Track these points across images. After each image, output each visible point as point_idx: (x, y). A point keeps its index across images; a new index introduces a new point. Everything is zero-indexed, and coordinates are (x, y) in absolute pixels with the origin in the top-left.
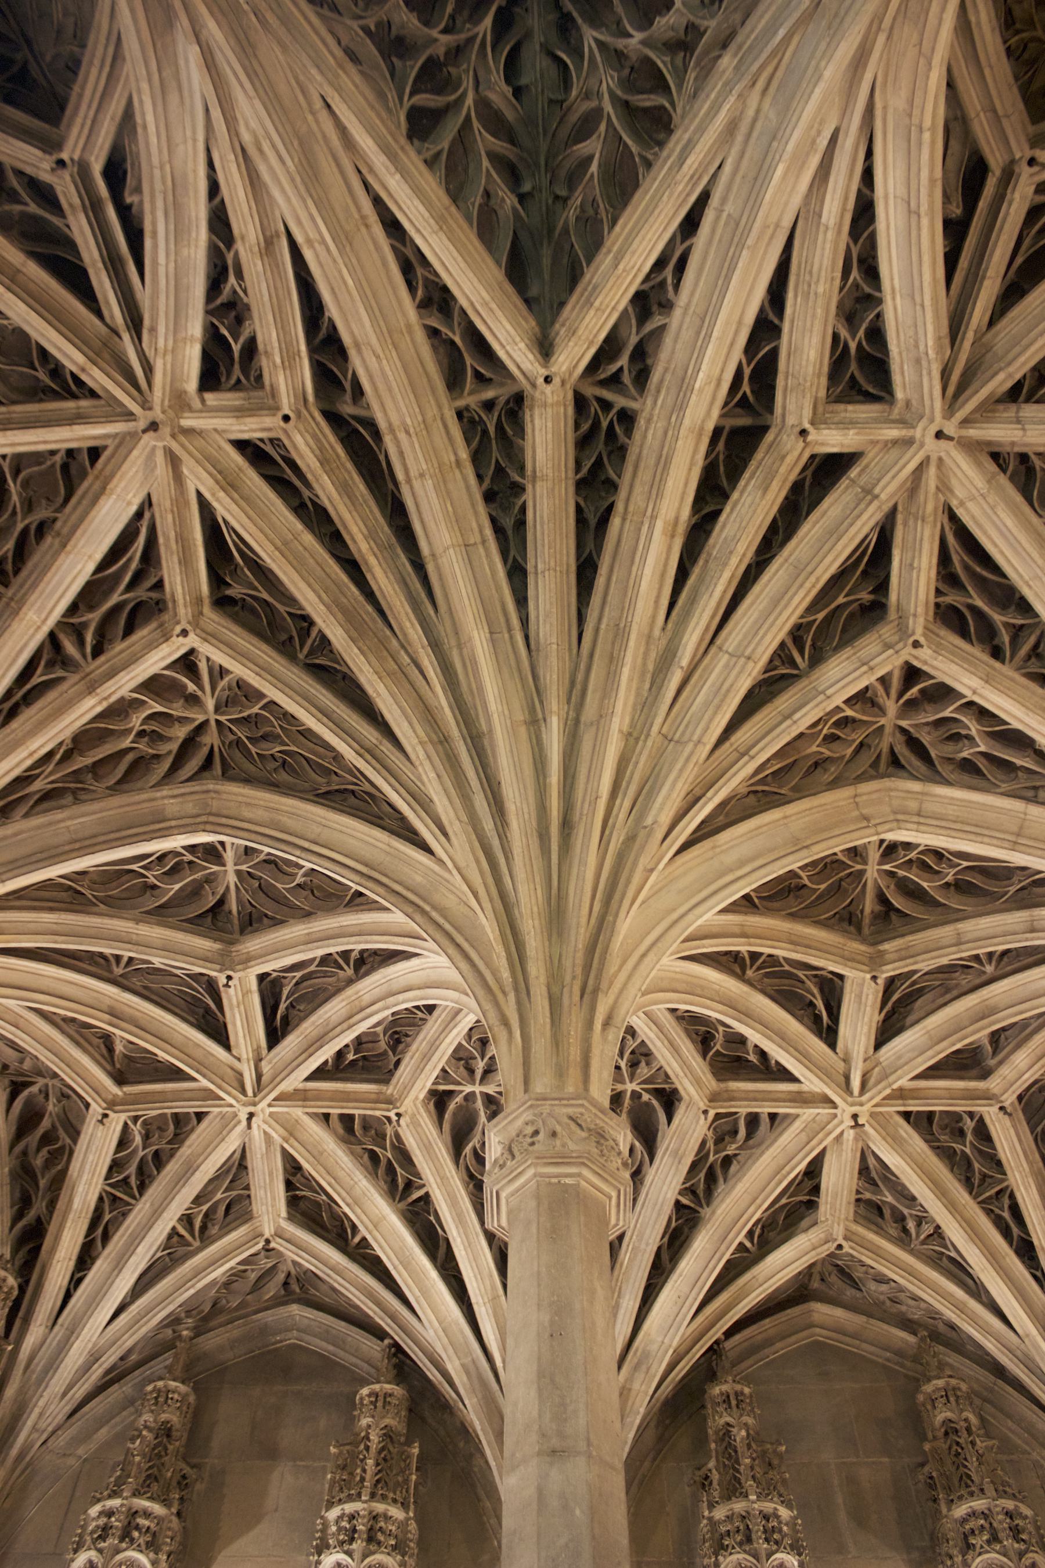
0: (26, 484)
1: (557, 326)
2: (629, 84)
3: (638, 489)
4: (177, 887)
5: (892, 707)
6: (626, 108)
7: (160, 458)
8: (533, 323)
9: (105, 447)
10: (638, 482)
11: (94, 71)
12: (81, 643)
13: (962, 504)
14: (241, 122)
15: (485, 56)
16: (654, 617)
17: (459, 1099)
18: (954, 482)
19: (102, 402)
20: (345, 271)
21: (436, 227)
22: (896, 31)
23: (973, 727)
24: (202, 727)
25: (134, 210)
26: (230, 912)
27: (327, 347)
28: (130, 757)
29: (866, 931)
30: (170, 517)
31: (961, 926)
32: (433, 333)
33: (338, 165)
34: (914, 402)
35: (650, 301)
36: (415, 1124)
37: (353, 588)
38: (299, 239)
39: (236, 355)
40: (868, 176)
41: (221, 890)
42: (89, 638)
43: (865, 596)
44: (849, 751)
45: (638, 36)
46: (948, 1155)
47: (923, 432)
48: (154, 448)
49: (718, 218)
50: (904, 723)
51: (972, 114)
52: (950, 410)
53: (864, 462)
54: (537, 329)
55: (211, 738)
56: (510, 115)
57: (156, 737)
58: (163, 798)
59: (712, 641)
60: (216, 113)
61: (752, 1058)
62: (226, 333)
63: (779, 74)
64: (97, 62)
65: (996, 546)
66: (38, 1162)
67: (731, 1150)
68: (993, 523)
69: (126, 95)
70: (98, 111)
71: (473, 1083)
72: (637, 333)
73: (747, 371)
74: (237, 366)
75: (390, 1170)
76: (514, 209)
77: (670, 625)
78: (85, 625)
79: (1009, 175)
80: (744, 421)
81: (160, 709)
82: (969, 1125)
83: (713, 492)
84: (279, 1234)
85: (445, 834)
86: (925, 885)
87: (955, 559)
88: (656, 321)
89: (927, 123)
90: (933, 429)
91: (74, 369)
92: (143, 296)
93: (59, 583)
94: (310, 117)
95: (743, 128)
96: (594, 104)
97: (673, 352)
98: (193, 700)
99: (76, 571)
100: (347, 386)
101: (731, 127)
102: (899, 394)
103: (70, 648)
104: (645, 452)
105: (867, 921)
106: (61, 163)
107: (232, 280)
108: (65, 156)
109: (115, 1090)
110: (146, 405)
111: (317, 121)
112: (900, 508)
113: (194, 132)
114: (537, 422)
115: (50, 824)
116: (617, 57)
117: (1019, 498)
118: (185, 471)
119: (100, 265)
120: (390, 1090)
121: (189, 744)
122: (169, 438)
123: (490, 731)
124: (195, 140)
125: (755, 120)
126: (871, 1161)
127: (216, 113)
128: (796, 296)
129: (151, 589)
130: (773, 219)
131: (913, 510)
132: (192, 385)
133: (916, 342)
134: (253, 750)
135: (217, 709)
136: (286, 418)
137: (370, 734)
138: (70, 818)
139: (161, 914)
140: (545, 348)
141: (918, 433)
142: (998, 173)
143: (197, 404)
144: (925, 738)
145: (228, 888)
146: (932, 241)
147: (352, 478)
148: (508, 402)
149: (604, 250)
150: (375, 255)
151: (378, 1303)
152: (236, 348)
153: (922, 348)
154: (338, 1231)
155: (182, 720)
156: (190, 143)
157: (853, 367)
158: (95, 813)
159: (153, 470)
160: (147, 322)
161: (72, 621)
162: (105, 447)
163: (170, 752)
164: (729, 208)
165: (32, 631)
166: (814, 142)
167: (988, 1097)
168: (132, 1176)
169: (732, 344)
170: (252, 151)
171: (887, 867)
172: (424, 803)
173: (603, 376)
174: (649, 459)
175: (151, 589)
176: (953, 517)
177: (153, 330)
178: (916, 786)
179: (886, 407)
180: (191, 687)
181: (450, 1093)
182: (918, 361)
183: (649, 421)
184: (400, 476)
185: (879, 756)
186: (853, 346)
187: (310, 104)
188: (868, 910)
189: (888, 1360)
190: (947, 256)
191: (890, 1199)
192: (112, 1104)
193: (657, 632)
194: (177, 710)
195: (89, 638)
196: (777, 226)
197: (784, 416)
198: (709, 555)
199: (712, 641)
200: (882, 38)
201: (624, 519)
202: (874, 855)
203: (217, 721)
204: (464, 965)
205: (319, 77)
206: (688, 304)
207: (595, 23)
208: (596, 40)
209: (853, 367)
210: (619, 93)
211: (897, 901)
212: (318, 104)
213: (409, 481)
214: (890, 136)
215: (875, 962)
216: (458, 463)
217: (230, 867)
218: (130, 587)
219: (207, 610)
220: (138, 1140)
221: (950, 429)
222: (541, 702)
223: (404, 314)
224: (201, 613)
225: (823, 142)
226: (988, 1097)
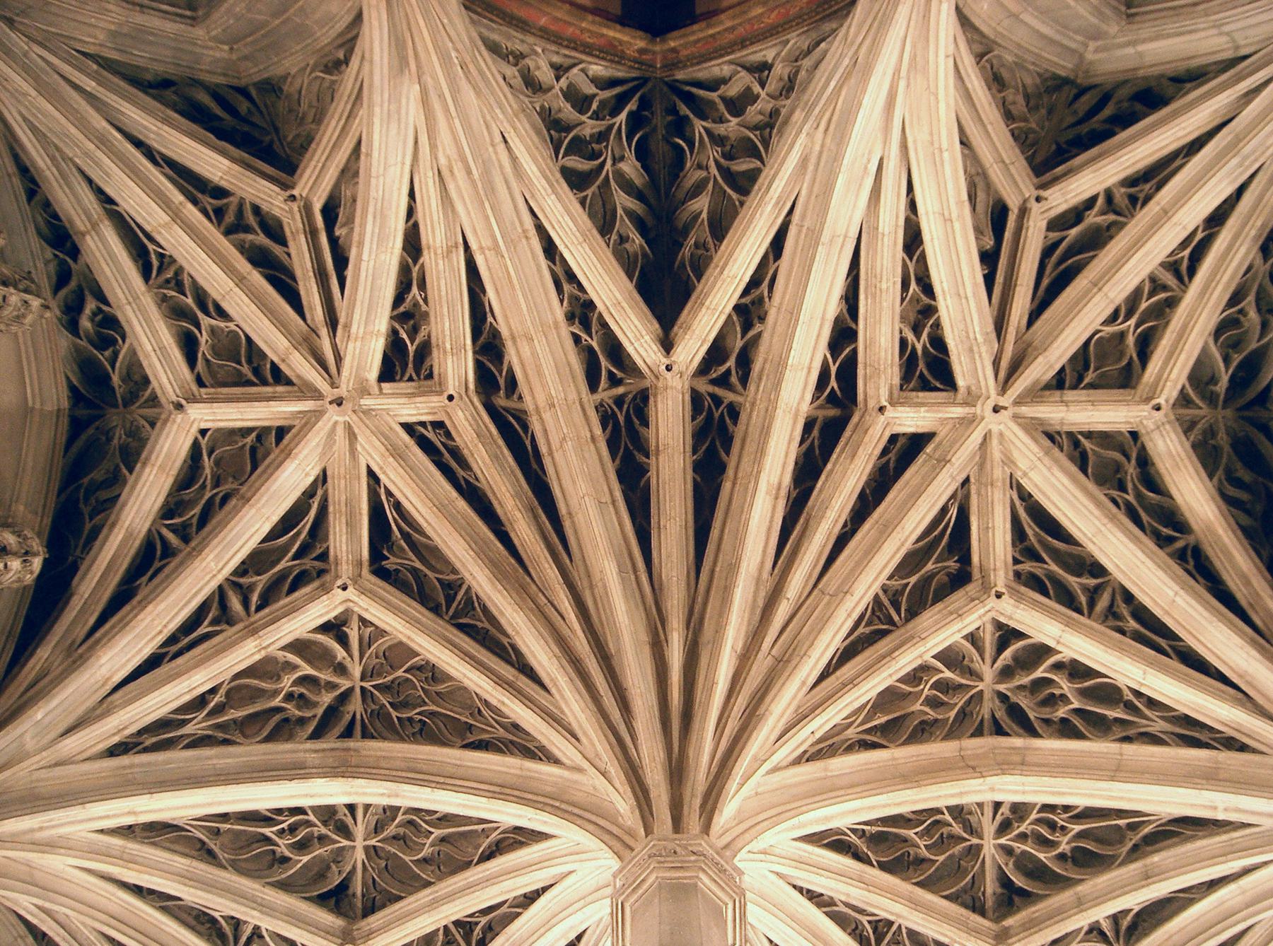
0: (217, 463)
1: (676, 328)
2: (729, 156)
3: (745, 459)
4: (305, 859)
5: (988, 673)
6: (728, 174)
7: (340, 431)
8: (657, 326)
9: (290, 428)
10: (745, 452)
11: (333, 123)
12: (246, 603)
13: (1025, 474)
14: (440, 148)
15: (621, 138)
16: (762, 563)
18: (1016, 455)
19: (296, 388)
20: (509, 263)
21: (581, 239)
22: (912, 81)
23: (1064, 685)
24: (345, 696)
25: (341, 241)
26: (354, 895)
27: (489, 346)
28: (277, 718)
29: (990, 913)
30: (343, 482)
31: (1079, 888)
32: (577, 339)
33: (509, 188)
34: (973, 388)
35: (749, 311)
37: (499, 545)
38: (474, 246)
39: (411, 354)
40: (912, 206)
41: (348, 868)
42: (255, 598)
43: (952, 564)
44: (953, 714)
45: (734, 121)
47: (984, 409)
48: (336, 423)
49: (800, 232)
50: (1002, 688)
51: (988, 165)
52: (1003, 389)
53: (937, 440)
54: (660, 331)
55: (355, 705)
57: (302, 701)
58: (306, 751)
59: (815, 586)
60: (423, 139)
62: (405, 336)
63: (835, 118)
64: (336, 117)
65: (1057, 507)
68: (1053, 486)
69: (357, 134)
70: (327, 159)
72: (742, 337)
73: (833, 369)
74: (411, 365)
76: (641, 246)
77: (776, 571)
78: (251, 588)
79: (1024, 211)
80: (833, 412)
81: (309, 670)
83: (809, 470)
85: (577, 739)
86: (1041, 856)
87: (1029, 532)
88: (758, 328)
89: (945, 145)
90: (990, 405)
91: (276, 360)
92: (341, 306)
93: (238, 536)
94: (491, 149)
95: (813, 160)
96: (704, 174)
97: (770, 345)
98: (341, 669)
99: (253, 530)
100: (502, 382)
101: (804, 162)
102: (961, 382)
103: (235, 604)
104: (750, 429)
105: (990, 903)
106: (293, 198)
107: (415, 290)
108: (296, 192)
110: (333, 385)
111: (496, 153)
112: (972, 480)
113: (404, 158)
114: (660, 405)
115: (198, 759)
116: (718, 140)
117: (1074, 469)
118: (359, 448)
119: (311, 274)
121: (332, 713)
122: (350, 413)
123: (619, 651)
124: (403, 164)
125: (821, 153)
127: (423, 139)
128: (866, 298)
129: (316, 559)
130: (841, 230)
131: (984, 480)
132: (373, 374)
133: (967, 332)
134: (394, 714)
135: (362, 680)
136: (451, 398)
137: (508, 672)
138: (217, 757)
139: (284, 886)
140: (667, 345)
141: (978, 410)
142: (1016, 211)
143: (376, 390)
144: (1024, 702)
145: (354, 868)
146: (973, 272)
147: (502, 452)
148: (635, 398)
149: (712, 265)
150: (532, 263)
152: (411, 349)
153: (972, 336)
155: (331, 686)
156: (399, 165)
157: (921, 366)
158: (240, 756)
159: (331, 447)
160: (342, 320)
161: (242, 580)
162: (290, 428)
163: (315, 716)
164: (807, 224)
165: (207, 578)
166: (866, 168)
169: (818, 336)
170: (445, 173)
171: (1003, 841)
172: (555, 719)
173: (714, 376)
174: (754, 433)
175: (316, 559)
176: (1025, 496)
177: (347, 326)
178: (1017, 742)
179: (951, 394)
180: (340, 653)
182: (971, 350)
183: (753, 404)
184: (543, 449)
185: (982, 721)
186: (919, 347)
187: (492, 140)
188: (989, 891)
190: (985, 276)
193: (765, 575)
194: (325, 676)
195: (255, 598)
197: (866, 400)
198: (809, 515)
199: (815, 586)
200: (902, 84)
201: (734, 484)
202: (989, 827)
203: (362, 688)
204: (591, 827)
205: (501, 116)
206: (781, 304)
207: (703, 117)
208: (705, 128)
209: (921, 366)
210: (722, 161)
211: (1019, 881)
212: (498, 139)
213: (551, 453)
214: (922, 164)
216: (593, 439)
217: (359, 843)
218: (295, 558)
219: (365, 571)
221: (1005, 401)
222: (664, 629)
223: (553, 314)
224: (360, 575)
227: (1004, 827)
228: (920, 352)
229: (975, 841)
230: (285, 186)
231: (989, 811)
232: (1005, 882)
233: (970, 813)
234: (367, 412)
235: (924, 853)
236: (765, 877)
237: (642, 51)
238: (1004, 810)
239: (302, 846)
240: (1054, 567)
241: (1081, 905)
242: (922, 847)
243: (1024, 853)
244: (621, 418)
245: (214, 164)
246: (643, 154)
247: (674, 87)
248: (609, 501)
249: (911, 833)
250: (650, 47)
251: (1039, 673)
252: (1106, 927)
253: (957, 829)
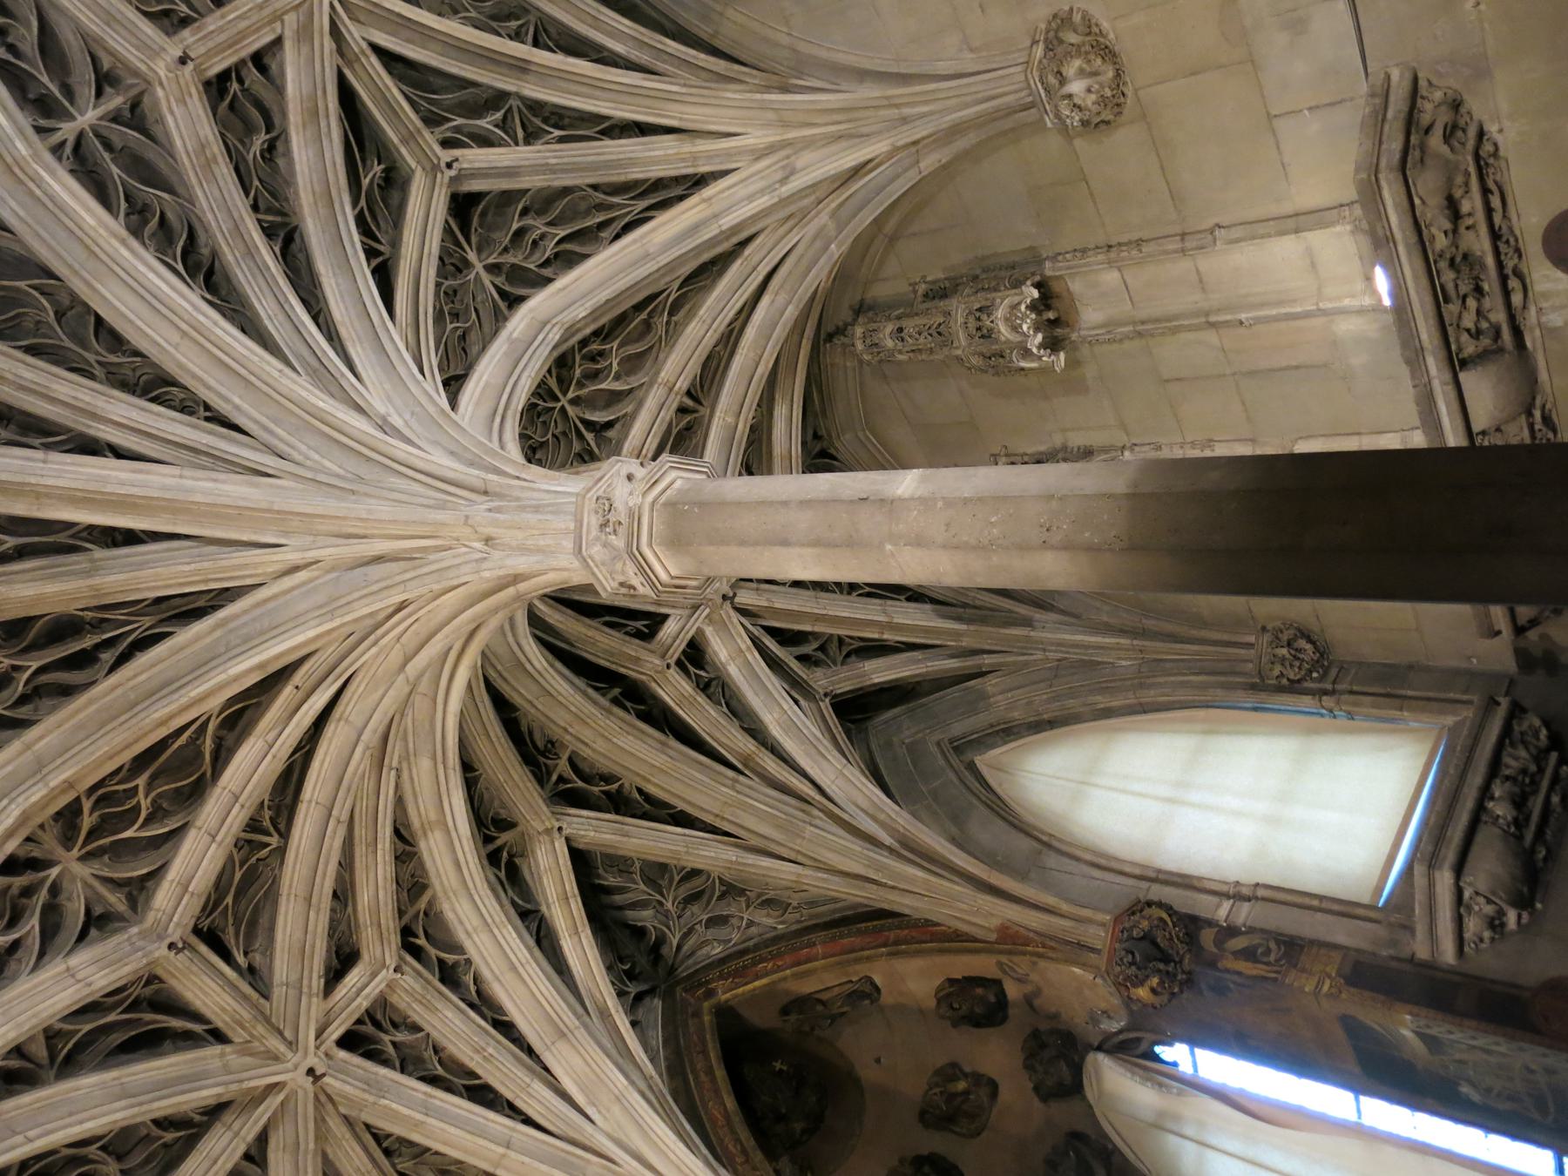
18: (248, 1060)
50: (54, 872)
56: (630, 914)
57: (593, 358)
71: (93, 127)
98: (575, 402)
102: (343, 1054)
112: (262, 1001)
155: (580, 385)
186: (386, 1038)
196: (548, 1048)
203: (558, 400)
225: (590, 1111)
228: (382, 1035)
230: (836, 696)
234: (696, 608)
236: (286, 534)
237: (710, 994)
239: (520, 233)
240: (112, 1017)
244: (542, 760)
245: (879, 672)
246: (639, 932)
247: (651, 992)
248: (536, 702)
250: (713, 1001)
251: (32, 925)
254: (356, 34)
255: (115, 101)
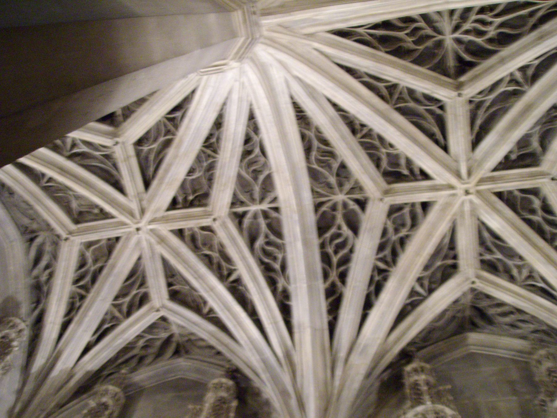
17: (249, 216)
36: (224, 225)
46: (529, 222)
61: (406, 172)
66: (44, 278)
67: (403, 232)
75: (219, 267)
82: (537, 203)
84: (164, 307)
109: (73, 227)
120: (208, 209)
126: (486, 234)
151: (217, 339)
154: (196, 305)
167: (543, 175)
168: (87, 279)
181: (244, 214)
189: (514, 356)
191: (499, 256)
192: (70, 233)
211: (467, 58)
215: (459, 87)
220: (90, 261)
226: (543, 175)
227: (457, 28)
229: (440, 37)
231: (446, 17)
232: (460, 59)
233: (437, 22)
235: (413, 46)
238: (456, 16)
241: (503, 61)
242: (409, 43)
243: (470, 42)
249: (401, 34)
252: (518, 76)
253: (429, 31)
254: (134, 206)
255: (240, 210)
